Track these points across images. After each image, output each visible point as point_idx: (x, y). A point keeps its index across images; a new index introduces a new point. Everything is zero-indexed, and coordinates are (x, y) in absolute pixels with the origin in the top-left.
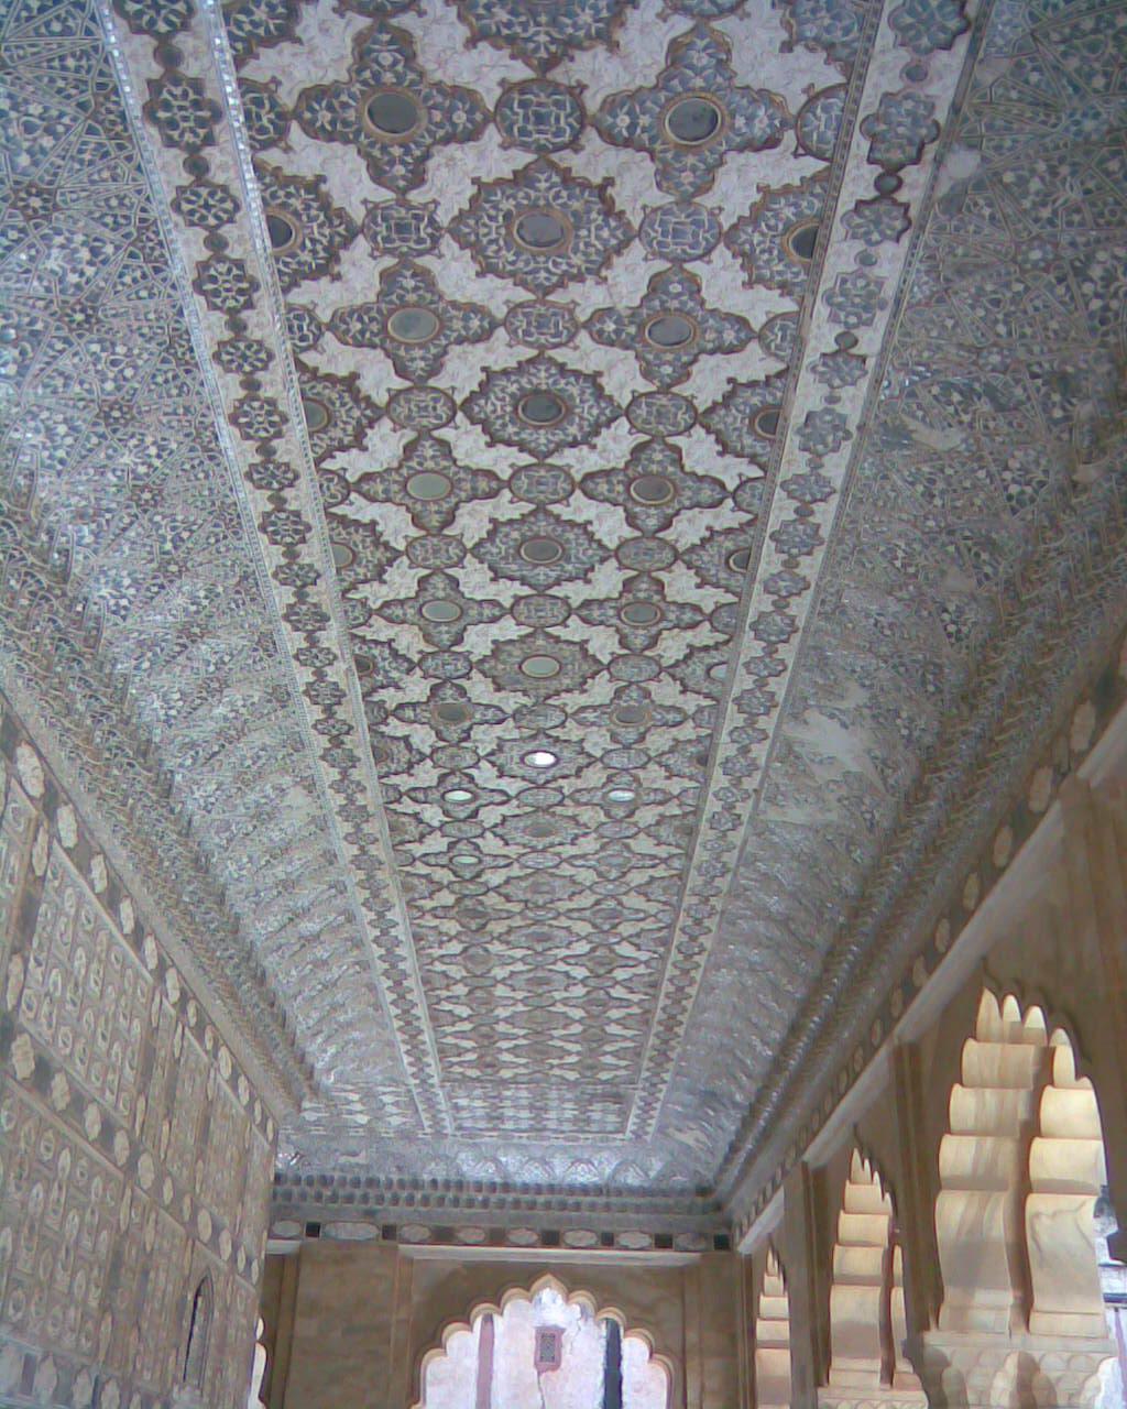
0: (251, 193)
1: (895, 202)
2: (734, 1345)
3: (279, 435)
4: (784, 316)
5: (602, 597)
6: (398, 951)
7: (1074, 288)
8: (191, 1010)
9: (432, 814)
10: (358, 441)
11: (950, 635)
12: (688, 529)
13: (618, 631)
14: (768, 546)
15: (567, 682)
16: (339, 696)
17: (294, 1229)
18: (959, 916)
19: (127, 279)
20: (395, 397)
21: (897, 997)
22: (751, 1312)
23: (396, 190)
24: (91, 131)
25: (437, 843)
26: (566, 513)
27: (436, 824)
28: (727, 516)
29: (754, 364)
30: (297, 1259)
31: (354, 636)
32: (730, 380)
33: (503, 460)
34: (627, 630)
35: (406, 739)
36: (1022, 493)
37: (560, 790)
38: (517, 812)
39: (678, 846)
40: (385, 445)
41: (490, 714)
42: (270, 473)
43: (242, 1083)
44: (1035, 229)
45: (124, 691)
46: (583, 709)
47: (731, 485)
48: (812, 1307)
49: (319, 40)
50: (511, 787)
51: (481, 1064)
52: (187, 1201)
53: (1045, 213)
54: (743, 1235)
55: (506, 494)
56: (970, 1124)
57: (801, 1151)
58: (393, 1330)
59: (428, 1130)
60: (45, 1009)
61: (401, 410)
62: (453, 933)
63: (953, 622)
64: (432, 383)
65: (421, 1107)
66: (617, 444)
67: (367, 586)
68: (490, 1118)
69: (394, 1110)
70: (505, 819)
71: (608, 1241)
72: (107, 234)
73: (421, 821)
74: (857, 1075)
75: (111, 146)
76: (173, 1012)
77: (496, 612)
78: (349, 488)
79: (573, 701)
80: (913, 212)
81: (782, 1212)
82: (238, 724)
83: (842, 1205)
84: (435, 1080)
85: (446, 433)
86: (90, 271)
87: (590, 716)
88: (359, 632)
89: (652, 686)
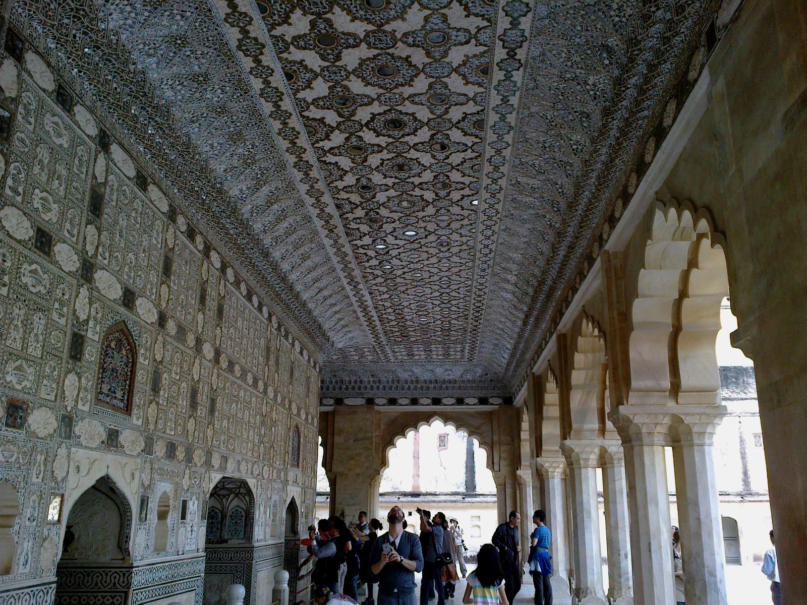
0: (277, 67)
1: (515, 59)
2: (513, 440)
3: (297, 138)
8: (282, 329)
9: (371, 253)
10: (327, 137)
11: (559, 192)
12: (456, 159)
13: (434, 192)
16: (331, 217)
17: (332, 402)
18: (575, 290)
19: (235, 97)
20: (339, 124)
23: (331, 62)
24: (218, 56)
25: (374, 262)
27: (373, 256)
28: (469, 154)
29: (471, 108)
30: (333, 413)
32: (464, 113)
33: (382, 141)
34: (437, 191)
35: (358, 229)
40: (338, 138)
41: (389, 220)
43: (305, 352)
44: (566, 68)
45: (248, 224)
46: (425, 217)
47: (470, 144)
48: (536, 427)
49: (298, 22)
52: (287, 400)
53: (569, 64)
54: (515, 398)
55: (385, 151)
56: (582, 365)
57: (532, 369)
60: (229, 343)
61: (343, 127)
64: (352, 118)
66: (424, 134)
69: (369, 354)
71: (460, 401)
72: (227, 84)
75: (226, 59)
76: (276, 332)
78: (325, 153)
79: (421, 214)
80: (522, 62)
82: (293, 229)
86: (221, 96)
87: (428, 219)
88: (336, 196)
89: (450, 208)
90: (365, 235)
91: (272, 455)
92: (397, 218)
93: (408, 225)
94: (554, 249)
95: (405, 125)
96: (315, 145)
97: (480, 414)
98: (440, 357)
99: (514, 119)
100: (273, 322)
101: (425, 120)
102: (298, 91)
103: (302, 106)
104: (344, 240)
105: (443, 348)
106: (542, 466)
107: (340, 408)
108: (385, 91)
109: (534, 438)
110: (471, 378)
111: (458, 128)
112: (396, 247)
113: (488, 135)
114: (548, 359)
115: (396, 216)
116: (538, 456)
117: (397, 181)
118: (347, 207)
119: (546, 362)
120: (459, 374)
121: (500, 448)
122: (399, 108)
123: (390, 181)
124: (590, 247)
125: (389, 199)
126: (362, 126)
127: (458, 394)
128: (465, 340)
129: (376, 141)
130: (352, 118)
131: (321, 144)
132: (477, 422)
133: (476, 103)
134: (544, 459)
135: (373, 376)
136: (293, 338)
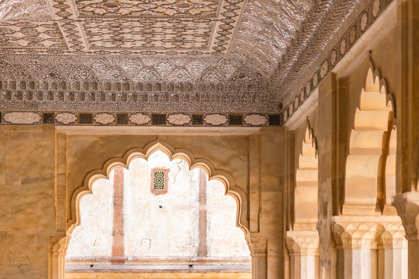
22: (293, 166)
48: (334, 167)
57: (331, 66)
58: (56, 180)
59: (71, 50)
65: (65, 34)
68: (114, 41)
69: (46, 36)
71: (198, 120)
74: (375, 18)
81: (317, 104)
84: (74, 17)
98: (168, 45)
105: (175, 28)
106: (342, 230)
109: (329, 182)
110: (217, 82)
114: (368, 48)
116: (335, 213)
119: (364, 55)
120: (197, 74)
121: (260, 196)
128: (214, 15)
132: (223, 154)
134: (346, 218)
135: (52, 75)
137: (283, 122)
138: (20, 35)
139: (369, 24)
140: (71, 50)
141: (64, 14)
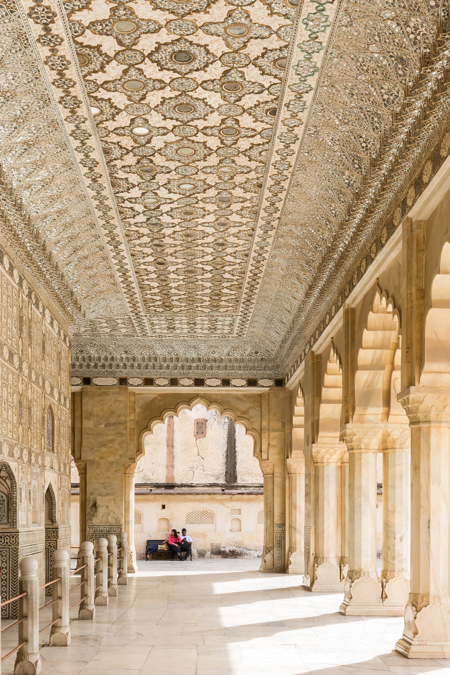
3: (66, 69)
4: (287, 26)
5: (212, 125)
6: (124, 261)
7: (404, 28)
9: (139, 208)
13: (219, 138)
14: (284, 108)
15: (198, 158)
17: (79, 381)
20: (117, 54)
21: (347, 287)
26: (195, 95)
27: (141, 211)
28: (265, 96)
30: (81, 393)
31: (102, 141)
36: (389, 98)
37: (196, 198)
38: (177, 206)
39: (250, 218)
40: (114, 70)
42: (62, 82)
43: (55, 323)
47: (267, 86)
50: (175, 197)
51: (164, 306)
55: (168, 88)
57: (311, 347)
59: (139, 335)
61: (121, 57)
62: (149, 253)
63: (364, 142)
64: (134, 47)
65: (135, 325)
66: (216, 71)
67: (108, 122)
68: (169, 328)
69: (123, 326)
70: (172, 210)
71: (226, 383)
73: (134, 210)
77: (165, 131)
79: (201, 164)
83: (325, 371)
85: (141, 66)
88: (104, 139)
89: (236, 159)
90: (134, 186)
91: (30, 438)
92: (173, 168)
93: (185, 176)
94: (350, 211)
95: (195, 58)
96: (87, 78)
97: (248, 397)
98: (206, 331)
99: (321, 59)
100: (24, 288)
101: (219, 54)
102: (73, 11)
103: (77, 30)
104: (107, 192)
105: (210, 320)
107: (87, 387)
108: (175, 17)
110: (239, 357)
111: (256, 65)
112: (169, 201)
113: (290, 76)
114: (331, 336)
115: (172, 165)
117: (178, 123)
118: (117, 152)
121: (269, 435)
122: (190, 38)
123: (169, 124)
124: (390, 211)
125: (167, 145)
126: (144, 57)
127: (223, 374)
129: (159, 75)
130: (134, 47)
131: (94, 76)
133: (279, 37)
136: (43, 306)
137: (285, 384)
138: (105, 325)
139: (330, 320)
140: (139, 335)
141: (136, 311)
